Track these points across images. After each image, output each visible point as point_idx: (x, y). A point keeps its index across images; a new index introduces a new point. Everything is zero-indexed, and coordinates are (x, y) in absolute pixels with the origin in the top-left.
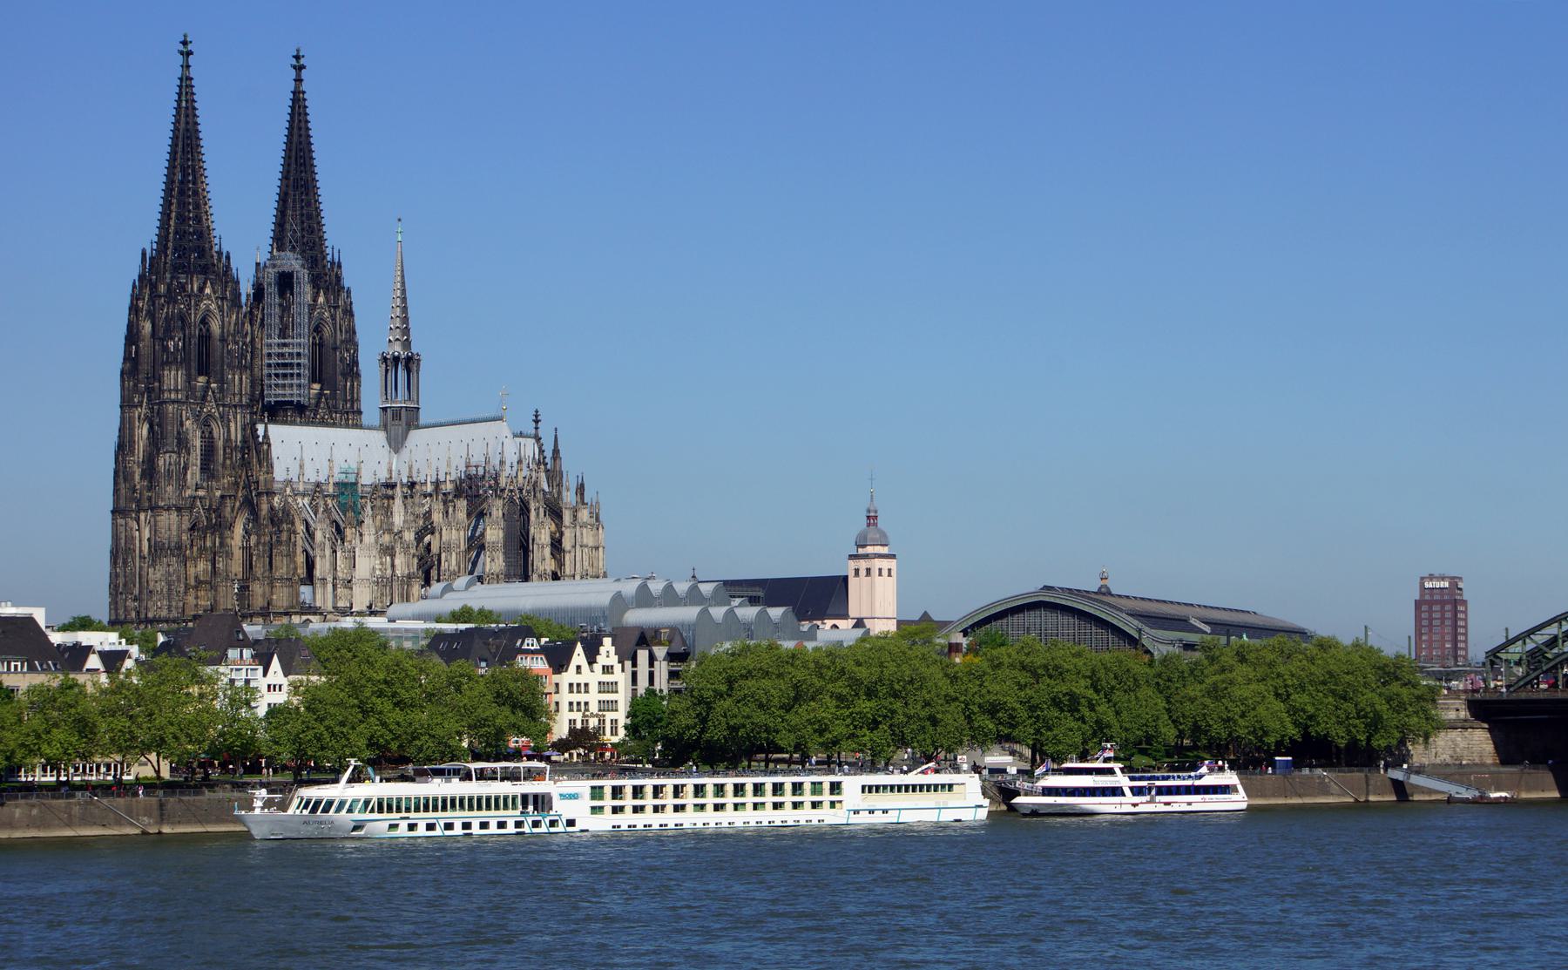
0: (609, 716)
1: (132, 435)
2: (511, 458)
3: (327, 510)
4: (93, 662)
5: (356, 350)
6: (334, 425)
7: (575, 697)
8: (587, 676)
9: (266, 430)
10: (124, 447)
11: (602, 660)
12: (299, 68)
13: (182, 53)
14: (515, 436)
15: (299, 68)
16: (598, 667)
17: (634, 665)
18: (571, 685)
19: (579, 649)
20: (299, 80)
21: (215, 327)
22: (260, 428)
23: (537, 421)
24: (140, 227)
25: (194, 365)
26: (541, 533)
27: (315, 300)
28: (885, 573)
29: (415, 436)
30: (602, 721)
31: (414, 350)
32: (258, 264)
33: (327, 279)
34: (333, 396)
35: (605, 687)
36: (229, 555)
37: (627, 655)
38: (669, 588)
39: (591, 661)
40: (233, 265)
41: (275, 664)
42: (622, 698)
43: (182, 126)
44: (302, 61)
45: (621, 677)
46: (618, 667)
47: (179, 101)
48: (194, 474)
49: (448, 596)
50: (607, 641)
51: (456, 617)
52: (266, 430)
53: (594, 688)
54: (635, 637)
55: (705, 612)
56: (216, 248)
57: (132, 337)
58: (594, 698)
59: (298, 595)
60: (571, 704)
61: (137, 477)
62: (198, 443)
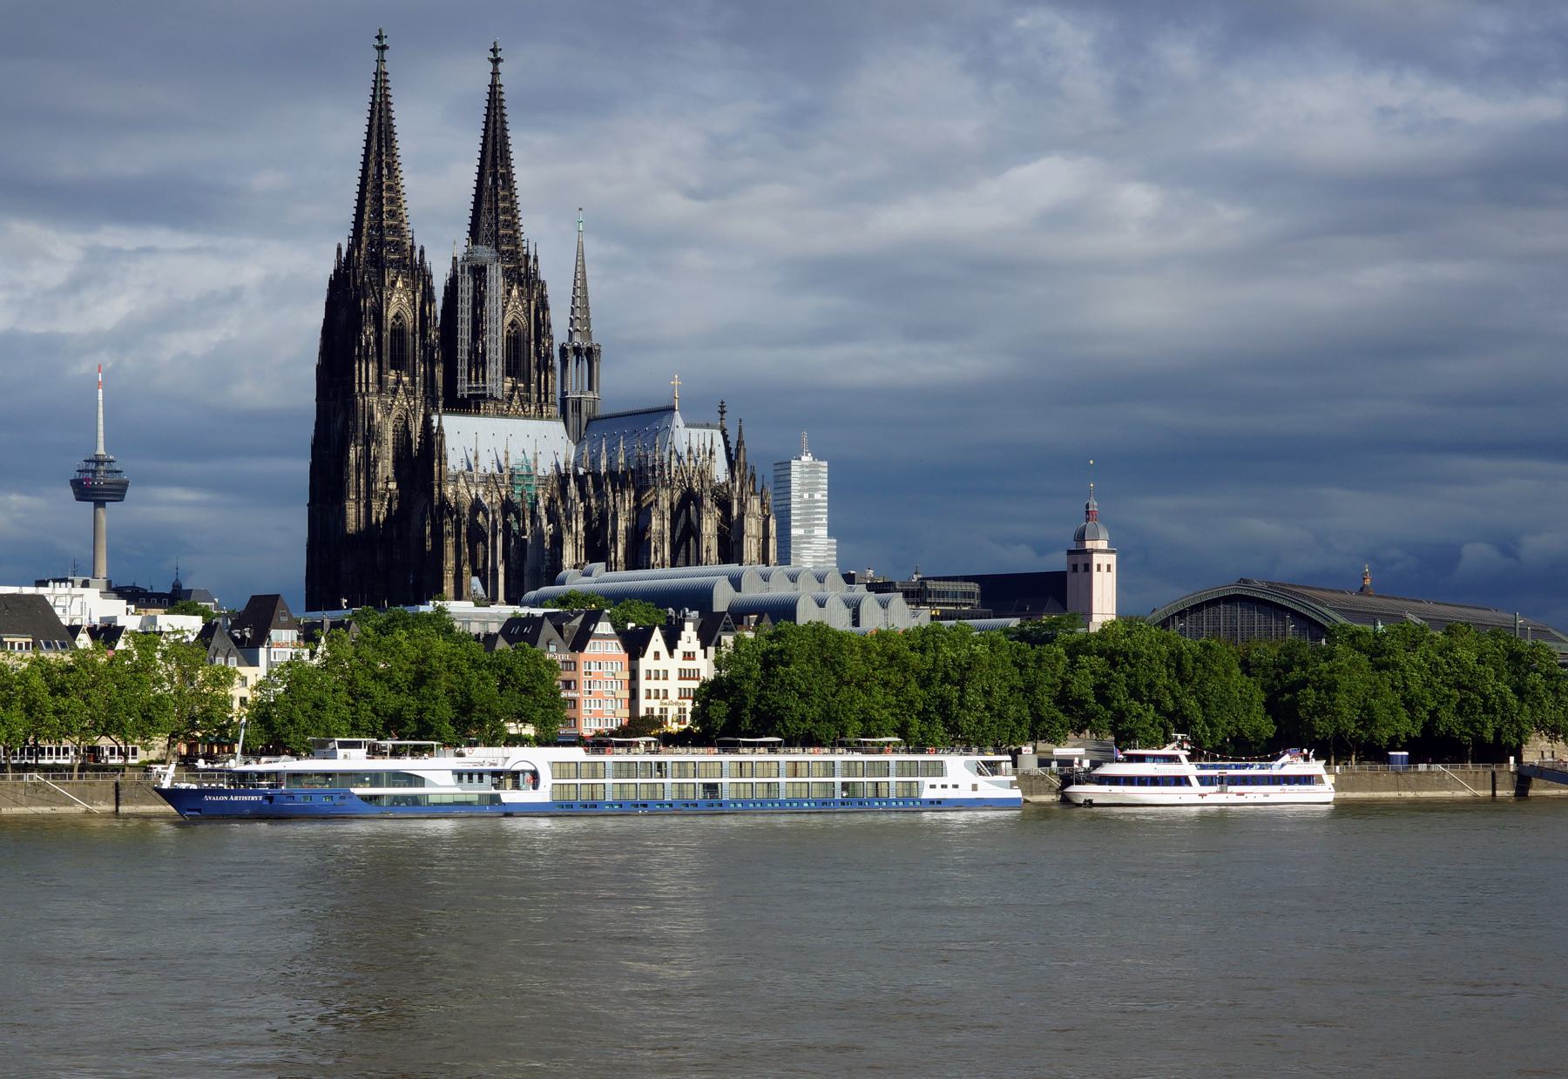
7: (653, 685)
8: (666, 662)
12: (496, 61)
14: (687, 426)
15: (496, 61)
16: (678, 653)
20: (495, 73)
22: (435, 418)
25: (386, 358)
26: (709, 527)
27: (509, 293)
28: (1104, 568)
33: (524, 276)
34: (528, 389)
39: (671, 645)
40: (427, 260)
43: (376, 121)
47: (374, 97)
48: (385, 467)
53: (673, 675)
56: (409, 243)
58: (674, 685)
62: (389, 436)
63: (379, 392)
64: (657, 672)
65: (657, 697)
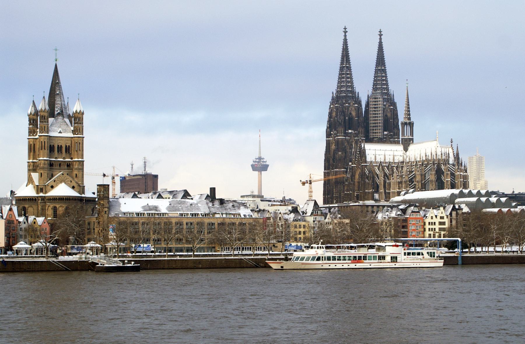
2: (439, 153)
7: (431, 227)
18: (429, 223)
21: (354, 114)
25: (347, 127)
31: (412, 120)
32: (368, 96)
36: (354, 184)
38: (479, 192)
40: (360, 96)
46: (445, 217)
53: (437, 224)
55: (479, 200)
58: (437, 227)
59: (373, 196)
60: (429, 229)
64: (432, 223)
65: (432, 230)
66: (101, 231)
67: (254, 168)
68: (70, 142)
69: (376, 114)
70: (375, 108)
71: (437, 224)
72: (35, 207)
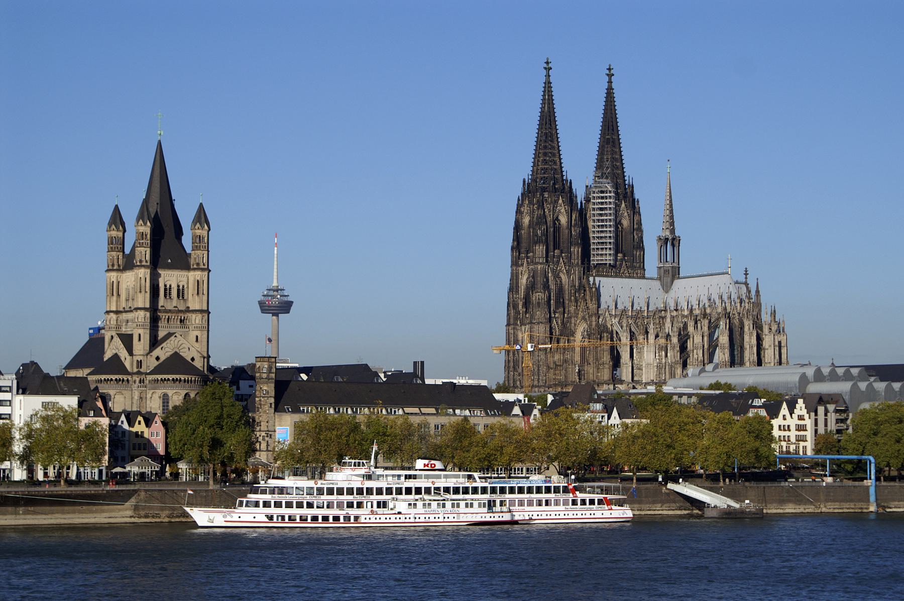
0: (802, 444)
1: (517, 283)
3: (629, 326)
4: (517, 410)
5: (642, 234)
6: (630, 277)
7: (782, 433)
9: (594, 280)
10: (513, 288)
11: (797, 412)
12: (610, 76)
13: (545, 68)
15: (610, 76)
17: (816, 415)
18: (780, 426)
19: (785, 405)
20: (610, 82)
21: (563, 220)
22: (591, 279)
23: (746, 274)
24: (522, 167)
26: (750, 340)
29: (676, 282)
30: (798, 447)
31: (677, 235)
32: (587, 186)
33: (625, 194)
35: (800, 428)
36: (573, 349)
37: (812, 409)
39: (791, 413)
41: (615, 413)
42: (809, 434)
44: (612, 72)
45: (808, 422)
46: (806, 416)
47: (544, 96)
49: (702, 375)
50: (800, 401)
51: (711, 387)
52: (594, 280)
53: (793, 428)
54: (817, 398)
55: (855, 387)
57: (518, 227)
58: (793, 434)
61: (520, 307)
63: (547, 261)
66: (264, 439)
67: (264, 308)
68: (185, 279)
69: (602, 221)
70: (601, 209)
71: (793, 428)
72: (127, 393)
